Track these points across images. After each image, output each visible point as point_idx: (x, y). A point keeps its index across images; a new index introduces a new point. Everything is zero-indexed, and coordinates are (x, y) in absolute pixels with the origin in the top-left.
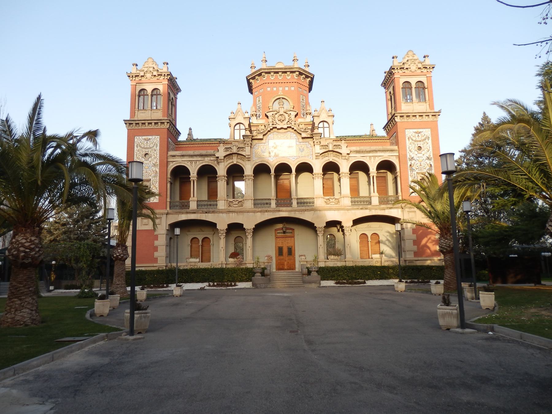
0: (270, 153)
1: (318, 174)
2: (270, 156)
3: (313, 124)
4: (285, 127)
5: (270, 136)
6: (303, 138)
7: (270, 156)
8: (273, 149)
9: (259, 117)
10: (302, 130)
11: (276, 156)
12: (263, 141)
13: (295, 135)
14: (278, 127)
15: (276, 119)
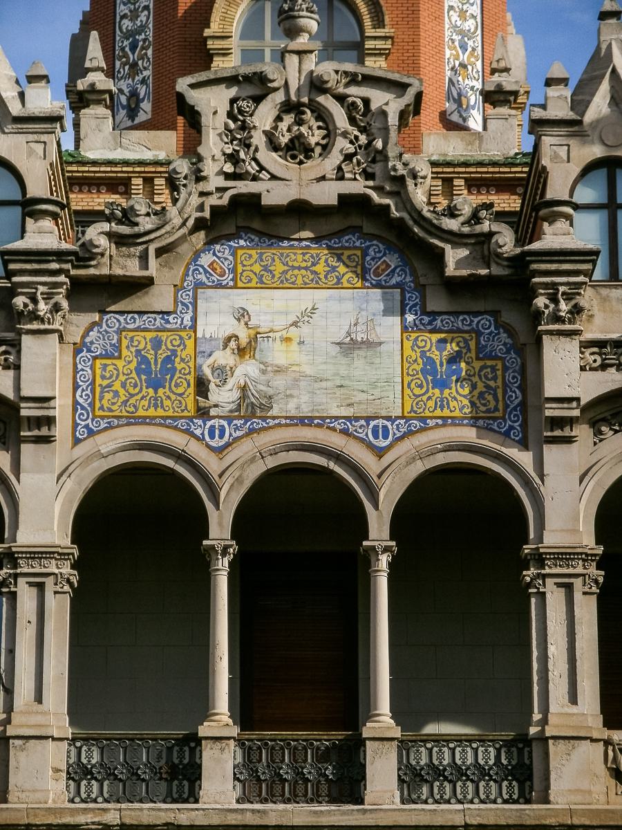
0: (202, 387)
1: (565, 556)
2: (203, 413)
3: (539, 176)
4: (326, 195)
5: (206, 259)
6: (455, 287)
7: (203, 413)
8: (224, 358)
9: (132, 112)
10: (452, 224)
11: (252, 409)
12: (160, 297)
13: (393, 260)
14: (275, 195)
15: (258, 139)
